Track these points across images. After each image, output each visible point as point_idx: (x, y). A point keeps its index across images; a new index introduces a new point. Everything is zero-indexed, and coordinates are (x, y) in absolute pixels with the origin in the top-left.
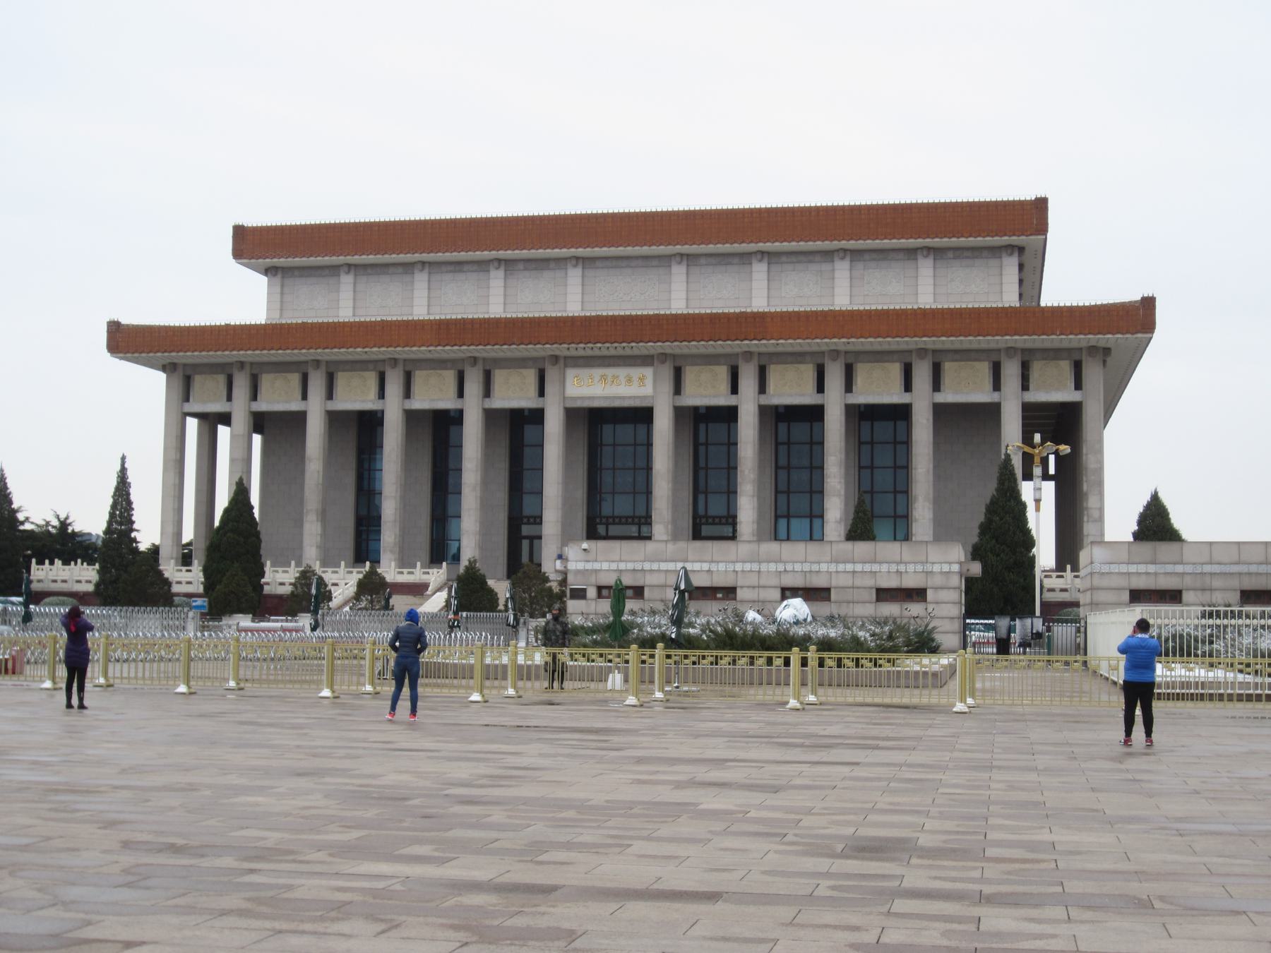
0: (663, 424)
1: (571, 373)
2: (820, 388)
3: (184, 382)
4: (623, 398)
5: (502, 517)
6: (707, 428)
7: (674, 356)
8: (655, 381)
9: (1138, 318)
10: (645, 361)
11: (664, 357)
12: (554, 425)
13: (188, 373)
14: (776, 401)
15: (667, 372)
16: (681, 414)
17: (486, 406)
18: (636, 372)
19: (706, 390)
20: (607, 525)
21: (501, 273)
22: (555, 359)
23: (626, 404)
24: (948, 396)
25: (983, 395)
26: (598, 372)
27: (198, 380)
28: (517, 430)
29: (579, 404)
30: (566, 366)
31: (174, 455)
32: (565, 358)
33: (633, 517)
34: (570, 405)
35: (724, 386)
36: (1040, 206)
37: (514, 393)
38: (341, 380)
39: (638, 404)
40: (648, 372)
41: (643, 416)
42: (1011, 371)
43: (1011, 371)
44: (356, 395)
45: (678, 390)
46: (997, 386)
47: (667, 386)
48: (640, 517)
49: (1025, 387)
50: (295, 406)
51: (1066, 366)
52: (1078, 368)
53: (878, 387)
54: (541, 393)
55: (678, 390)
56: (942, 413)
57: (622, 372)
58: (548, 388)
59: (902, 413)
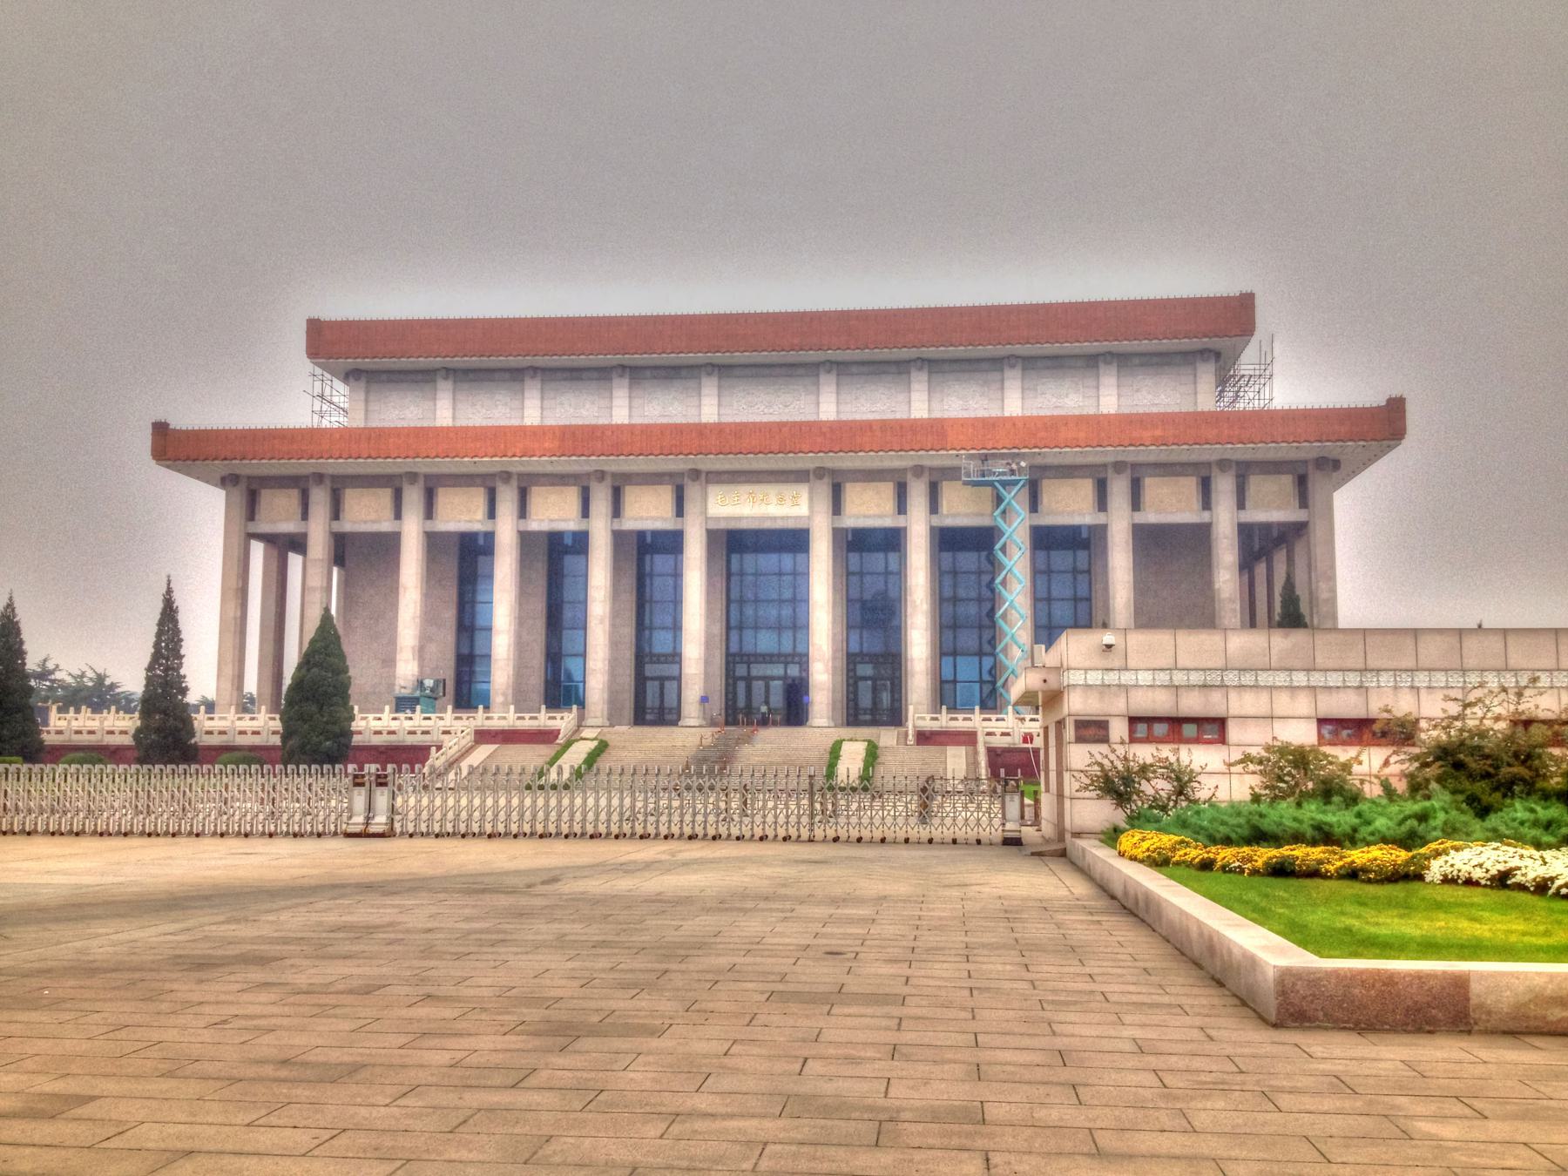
3: (249, 494)
4: (775, 519)
5: (628, 654)
6: (869, 550)
7: (833, 472)
8: (811, 499)
10: (799, 476)
11: (820, 473)
13: (254, 486)
14: (949, 522)
15: (824, 489)
17: (616, 527)
18: (789, 490)
19: (869, 507)
20: (749, 664)
21: (626, 381)
22: (695, 474)
23: (779, 525)
24: (1150, 517)
26: (744, 490)
28: (647, 555)
29: (723, 525)
30: (708, 482)
31: (234, 582)
32: (708, 473)
33: (779, 655)
34: (712, 526)
35: (889, 505)
37: (648, 510)
39: (791, 525)
40: (803, 491)
41: (794, 541)
42: (1224, 486)
43: (1224, 486)
45: (837, 508)
46: (1207, 504)
47: (824, 505)
48: (786, 656)
49: (1241, 505)
50: (386, 526)
51: (1287, 481)
52: (1302, 482)
54: (680, 512)
55: (837, 508)
57: (772, 491)
58: (691, 508)
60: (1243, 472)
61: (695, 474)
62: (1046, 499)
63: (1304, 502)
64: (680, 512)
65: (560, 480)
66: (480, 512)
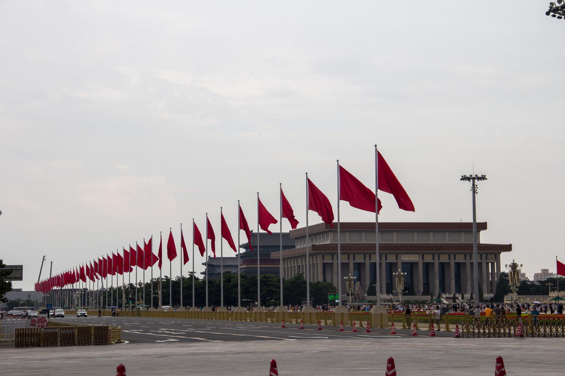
0: (421, 266)
1: (402, 255)
6: (428, 266)
9: (508, 248)
12: (400, 265)
15: (421, 256)
18: (415, 256)
19: (428, 259)
22: (399, 253)
27: (325, 255)
28: (391, 267)
36: (486, 223)
40: (417, 256)
42: (484, 256)
43: (484, 256)
47: (421, 258)
50: (347, 261)
52: (496, 256)
54: (397, 259)
57: (412, 255)
61: (399, 253)
64: (397, 259)
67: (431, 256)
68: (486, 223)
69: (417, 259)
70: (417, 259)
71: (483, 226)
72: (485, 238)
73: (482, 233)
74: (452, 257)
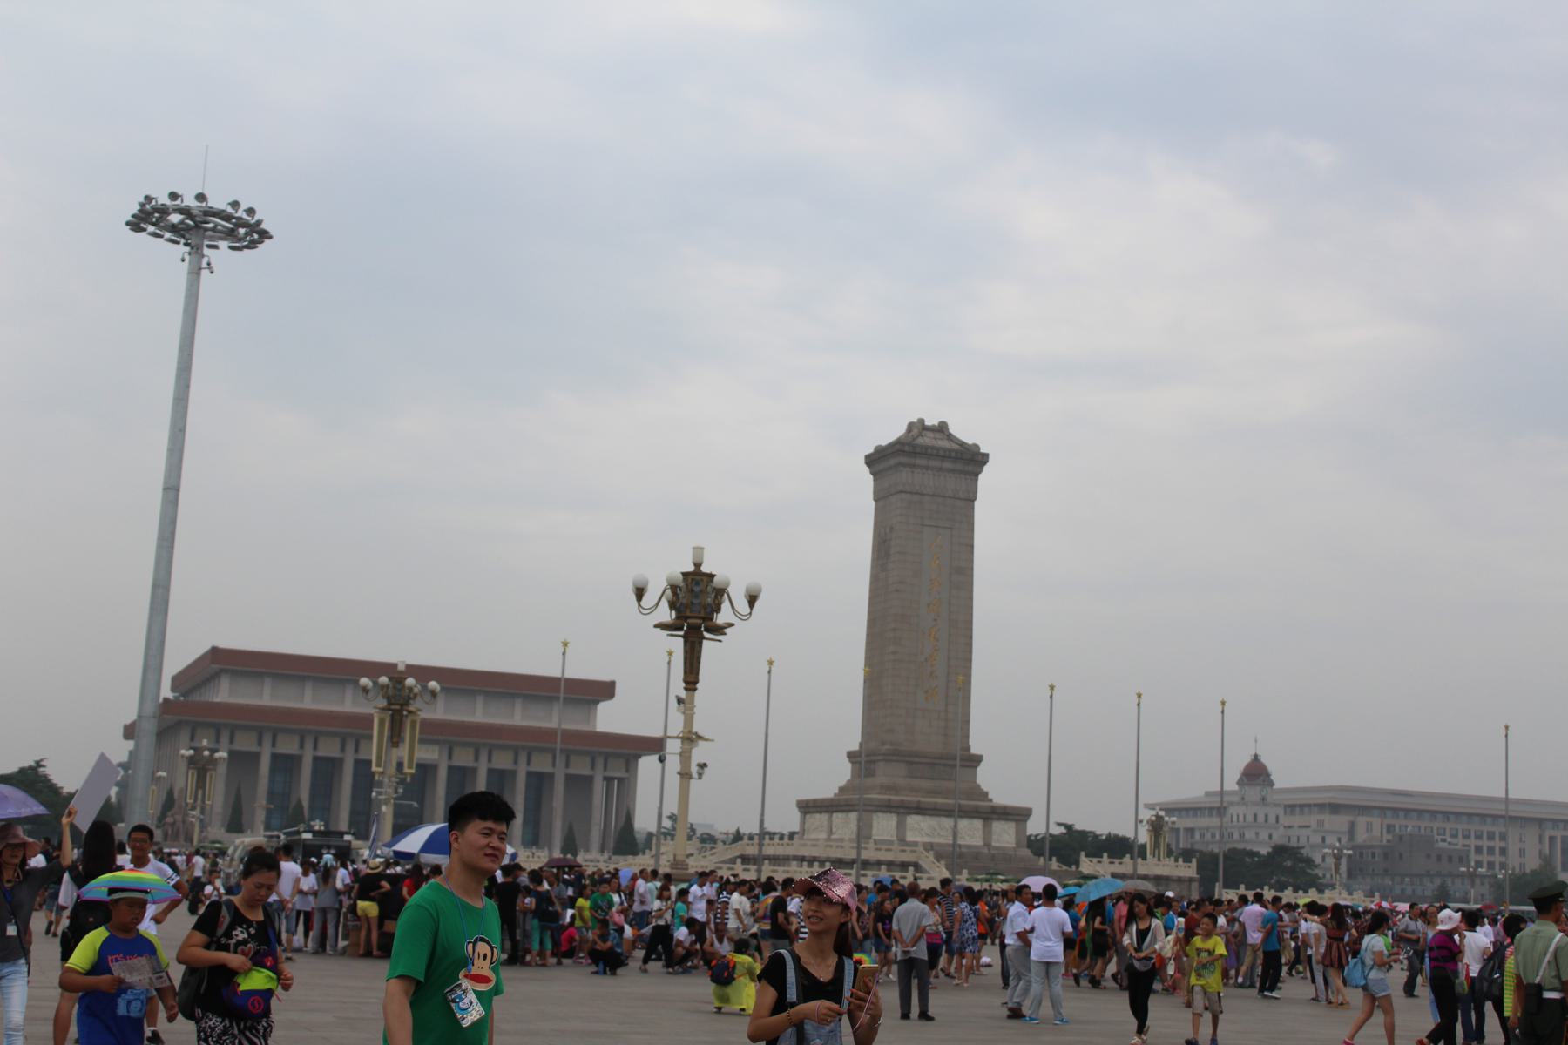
0: (443, 774)
2: (516, 762)
16: (451, 769)
24: (572, 771)
25: (586, 772)
35: (471, 757)
38: (280, 737)
42: (600, 762)
43: (600, 762)
44: (288, 746)
46: (593, 767)
50: (254, 748)
53: (541, 764)
55: (450, 757)
56: (569, 778)
59: (551, 776)
60: (607, 757)
62: (534, 758)
63: (627, 771)
65: (335, 734)
66: (296, 746)
67: (471, 751)
68: (612, 685)
69: (436, 756)
70: (436, 756)
71: (606, 690)
72: (609, 719)
73: (603, 708)
74: (523, 759)
